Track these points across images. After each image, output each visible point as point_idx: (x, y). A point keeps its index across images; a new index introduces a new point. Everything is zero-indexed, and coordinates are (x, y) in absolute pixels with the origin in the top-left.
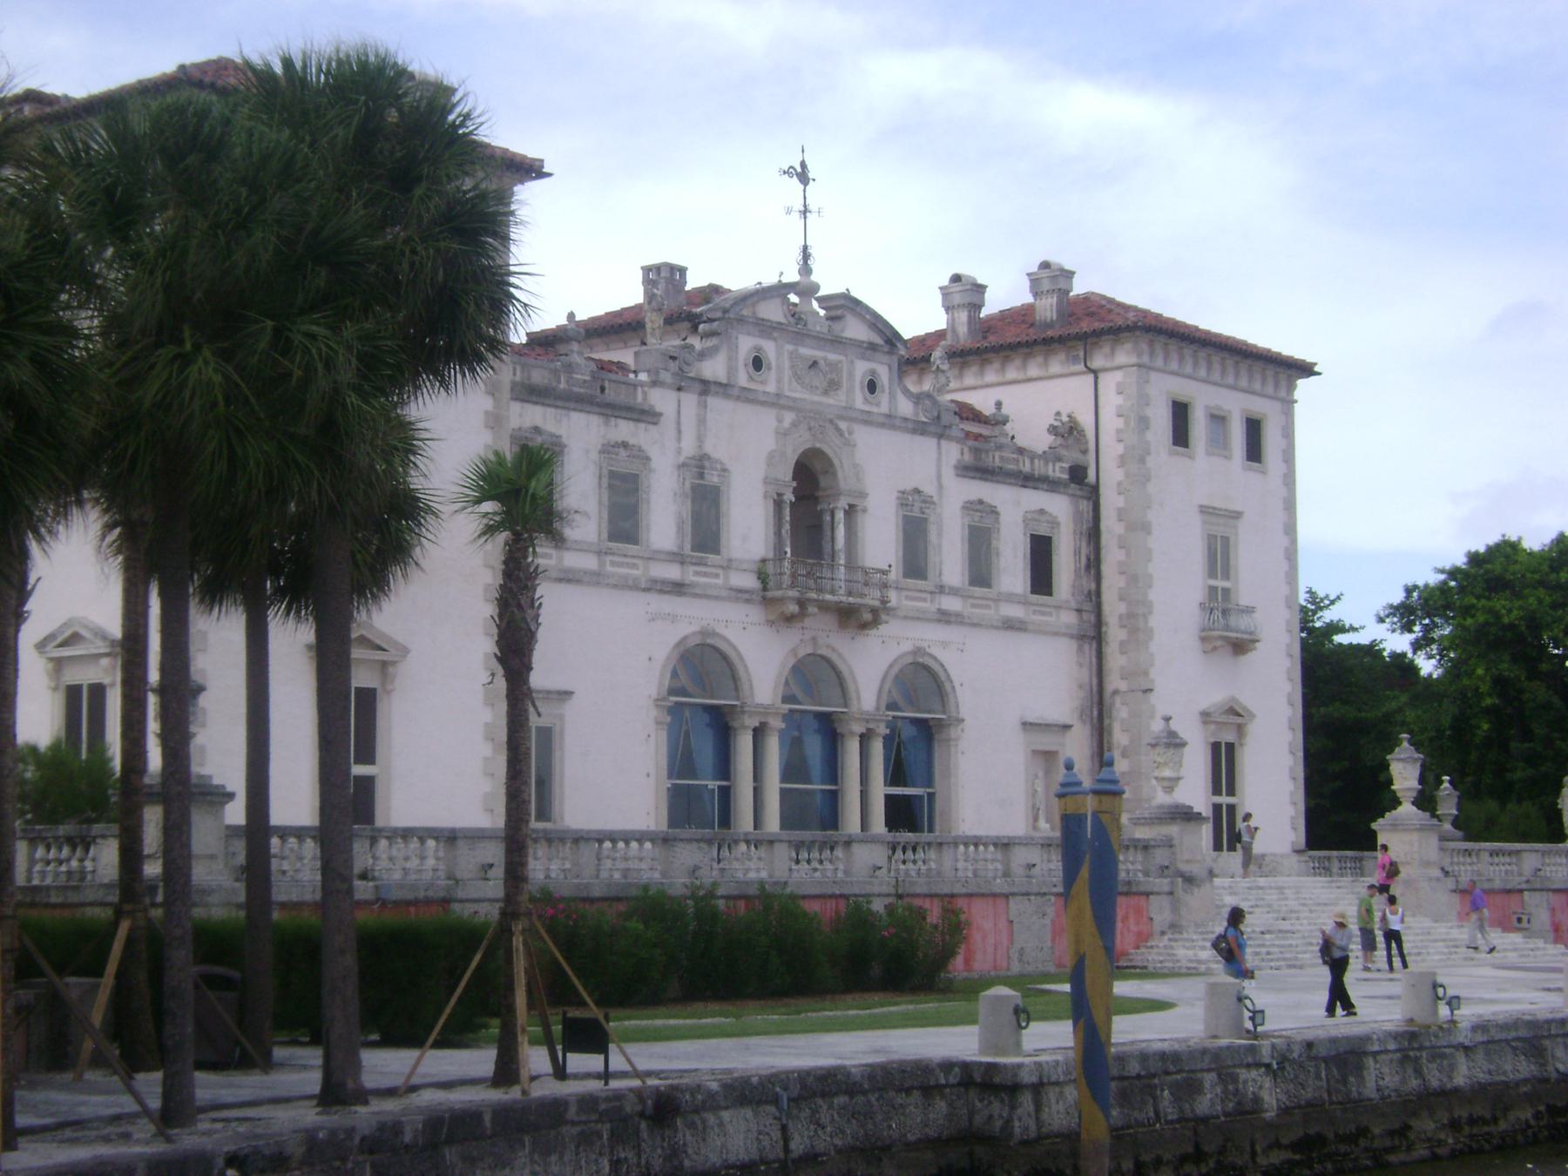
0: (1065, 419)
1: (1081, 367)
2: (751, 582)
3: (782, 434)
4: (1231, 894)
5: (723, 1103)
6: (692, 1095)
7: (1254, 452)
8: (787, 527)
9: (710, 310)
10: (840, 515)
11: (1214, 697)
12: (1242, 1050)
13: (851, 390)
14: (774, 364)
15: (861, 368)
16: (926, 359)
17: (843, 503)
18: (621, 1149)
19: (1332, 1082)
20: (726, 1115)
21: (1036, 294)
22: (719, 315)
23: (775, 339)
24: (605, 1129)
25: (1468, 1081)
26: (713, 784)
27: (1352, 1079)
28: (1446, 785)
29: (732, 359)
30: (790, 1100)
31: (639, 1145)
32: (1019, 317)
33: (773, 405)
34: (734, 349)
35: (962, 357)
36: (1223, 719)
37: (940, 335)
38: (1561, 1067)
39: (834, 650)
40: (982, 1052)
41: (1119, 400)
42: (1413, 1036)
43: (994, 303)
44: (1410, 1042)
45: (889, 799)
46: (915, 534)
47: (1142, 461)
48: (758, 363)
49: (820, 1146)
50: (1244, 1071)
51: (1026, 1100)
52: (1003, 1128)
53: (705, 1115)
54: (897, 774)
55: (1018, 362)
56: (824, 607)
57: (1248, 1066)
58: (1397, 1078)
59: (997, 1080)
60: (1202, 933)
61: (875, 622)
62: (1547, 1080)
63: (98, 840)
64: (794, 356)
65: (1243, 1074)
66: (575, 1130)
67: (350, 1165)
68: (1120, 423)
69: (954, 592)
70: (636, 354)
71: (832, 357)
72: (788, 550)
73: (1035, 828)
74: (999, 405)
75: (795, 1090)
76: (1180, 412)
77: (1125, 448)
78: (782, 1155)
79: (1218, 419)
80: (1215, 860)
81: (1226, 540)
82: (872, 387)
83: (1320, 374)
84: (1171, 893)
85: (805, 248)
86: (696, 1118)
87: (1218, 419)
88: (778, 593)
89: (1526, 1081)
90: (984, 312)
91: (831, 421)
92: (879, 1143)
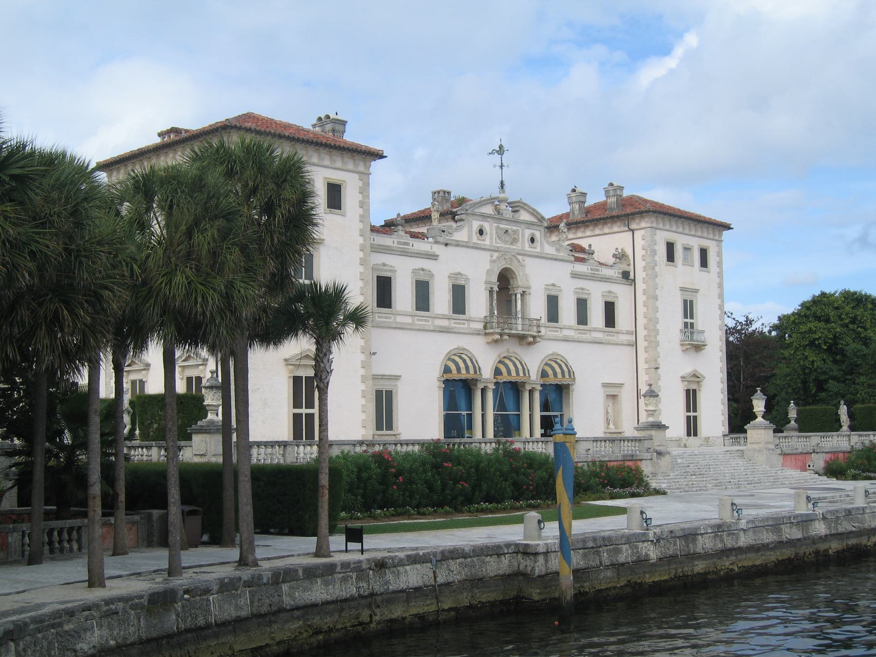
0: (620, 251)
1: (626, 228)
2: (480, 326)
3: (493, 262)
4: (681, 458)
5: (407, 563)
6: (393, 560)
7: (704, 263)
8: (495, 302)
9: (461, 209)
10: (519, 296)
11: (687, 370)
12: (640, 535)
13: (523, 242)
14: (489, 233)
15: (528, 233)
16: (557, 227)
17: (520, 291)
18: (360, 583)
19: (681, 547)
20: (408, 568)
21: (607, 197)
22: (464, 212)
23: (488, 222)
24: (354, 575)
25: (745, 544)
26: (464, 413)
27: (691, 545)
28: (792, 404)
29: (470, 231)
30: (436, 561)
31: (369, 581)
32: (602, 206)
33: (488, 250)
34: (471, 227)
35: (574, 225)
36: (691, 379)
37: (568, 215)
38: (788, 536)
39: (517, 354)
40: (525, 539)
41: (643, 242)
42: (719, 526)
43: (590, 201)
44: (718, 529)
45: (542, 417)
46: (553, 303)
47: (653, 269)
48: (481, 232)
49: (451, 579)
50: (641, 543)
51: (541, 559)
52: (531, 570)
53: (399, 568)
54: (545, 406)
55: (600, 226)
56: (510, 335)
57: (643, 541)
58: (712, 544)
59: (528, 551)
60: (664, 476)
61: (534, 342)
62: (782, 542)
63: (184, 448)
64: (498, 228)
65: (640, 545)
66: (340, 576)
67: (239, 592)
68: (644, 252)
69: (570, 328)
70: (428, 230)
71: (514, 228)
72: (496, 312)
73: (608, 428)
74: (590, 246)
75: (439, 557)
76: (670, 247)
77: (646, 263)
78: (433, 583)
79: (687, 249)
80: (687, 440)
81: (691, 302)
82: (532, 240)
83: (733, 229)
84: (651, 459)
85: (502, 182)
86: (395, 569)
87: (687, 249)
88: (491, 331)
89: (772, 543)
90: (586, 205)
91: (514, 255)
92: (477, 578)
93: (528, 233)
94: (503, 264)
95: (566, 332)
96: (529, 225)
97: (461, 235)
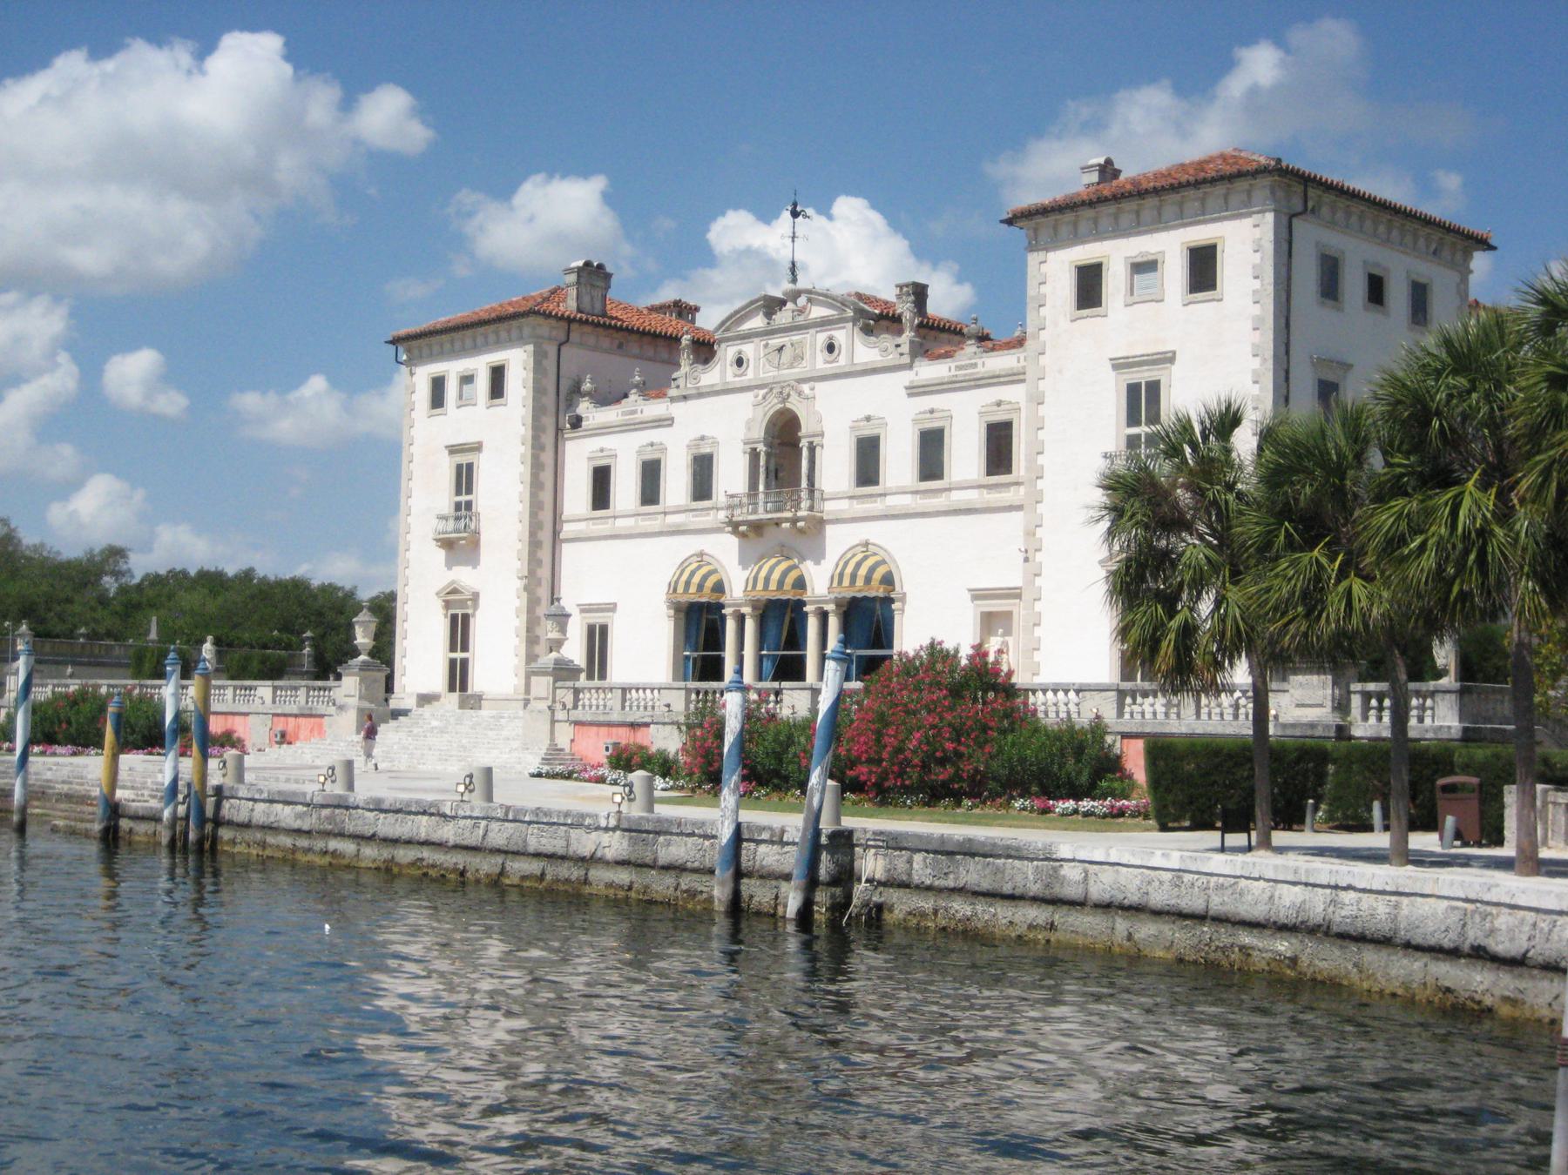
15: (822, 338)
69: (903, 492)
71: (794, 338)
85: (793, 264)
93: (822, 338)
94: (774, 405)
95: (959, 497)
96: (824, 323)
97: (711, 376)
